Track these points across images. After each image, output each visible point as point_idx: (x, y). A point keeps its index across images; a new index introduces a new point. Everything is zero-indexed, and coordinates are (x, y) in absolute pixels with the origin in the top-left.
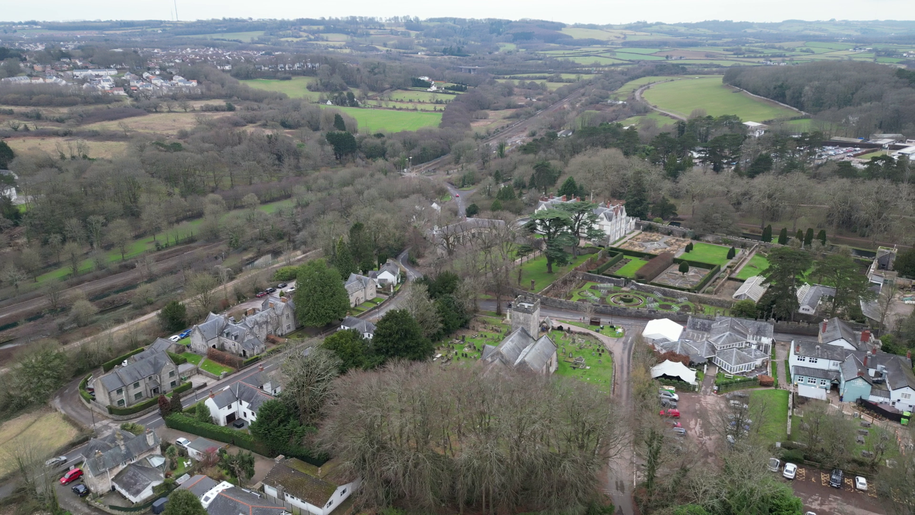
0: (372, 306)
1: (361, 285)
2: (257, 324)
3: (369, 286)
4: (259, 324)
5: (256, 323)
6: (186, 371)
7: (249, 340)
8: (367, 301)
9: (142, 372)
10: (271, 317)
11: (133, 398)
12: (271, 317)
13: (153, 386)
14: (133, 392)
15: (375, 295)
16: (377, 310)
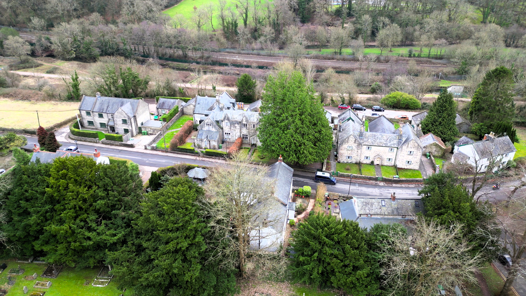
0: (392, 175)
1: (395, 142)
2: (228, 119)
3: (406, 149)
4: (233, 123)
5: (227, 118)
6: (149, 127)
7: (209, 131)
8: (395, 166)
9: (109, 109)
10: (247, 121)
11: (99, 126)
12: (247, 121)
13: (111, 124)
14: (98, 121)
15: (415, 166)
16: (382, 184)
